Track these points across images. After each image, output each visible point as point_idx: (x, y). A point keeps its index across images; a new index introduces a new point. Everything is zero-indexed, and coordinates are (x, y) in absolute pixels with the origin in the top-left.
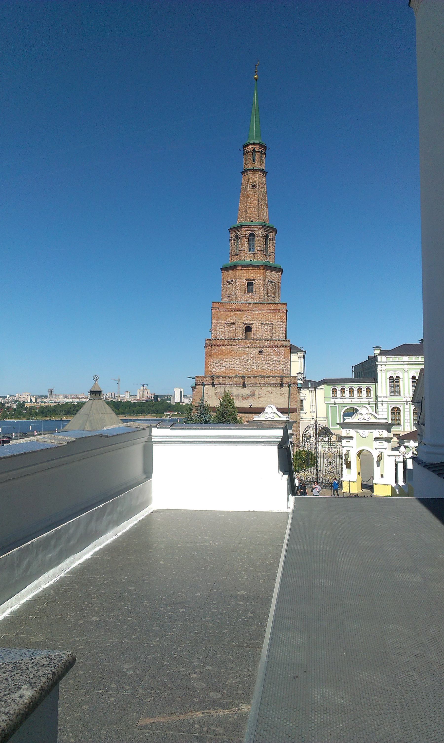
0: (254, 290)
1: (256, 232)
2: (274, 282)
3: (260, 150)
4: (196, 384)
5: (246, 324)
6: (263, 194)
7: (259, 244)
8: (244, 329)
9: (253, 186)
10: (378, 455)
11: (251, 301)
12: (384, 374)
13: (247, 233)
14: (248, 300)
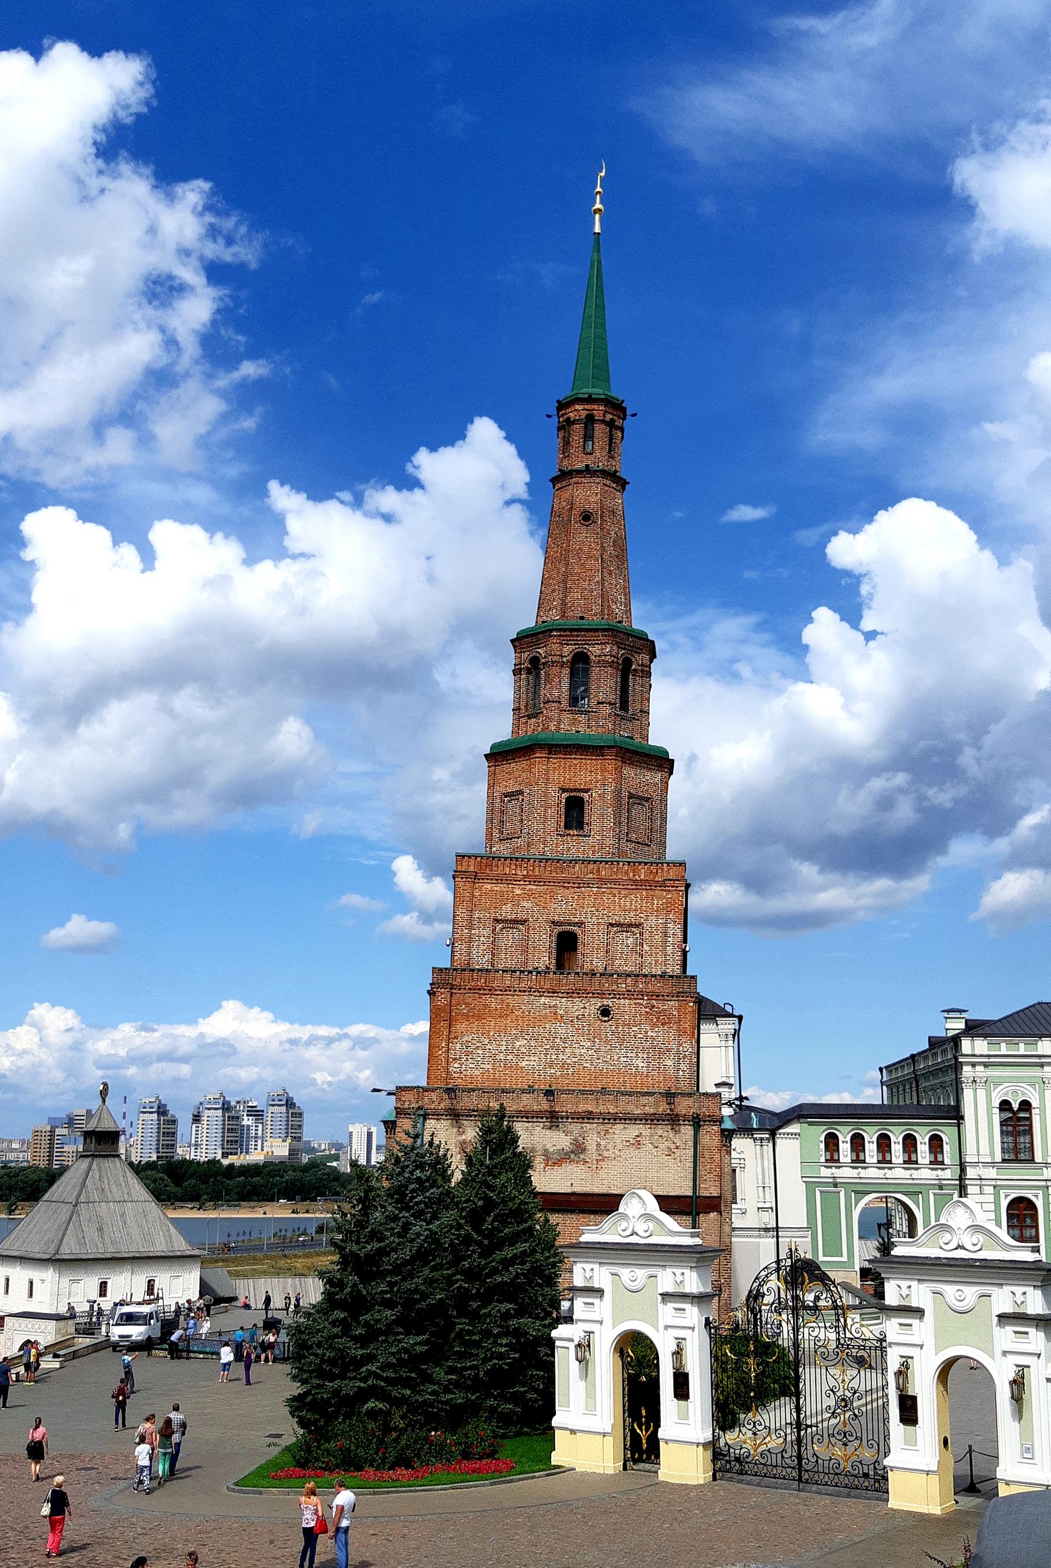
1: (594, 651)
4: (399, 1112)
6: (614, 541)
9: (587, 517)
10: (1011, 1376)
12: (981, 1093)
13: (567, 650)
14: (569, 849)
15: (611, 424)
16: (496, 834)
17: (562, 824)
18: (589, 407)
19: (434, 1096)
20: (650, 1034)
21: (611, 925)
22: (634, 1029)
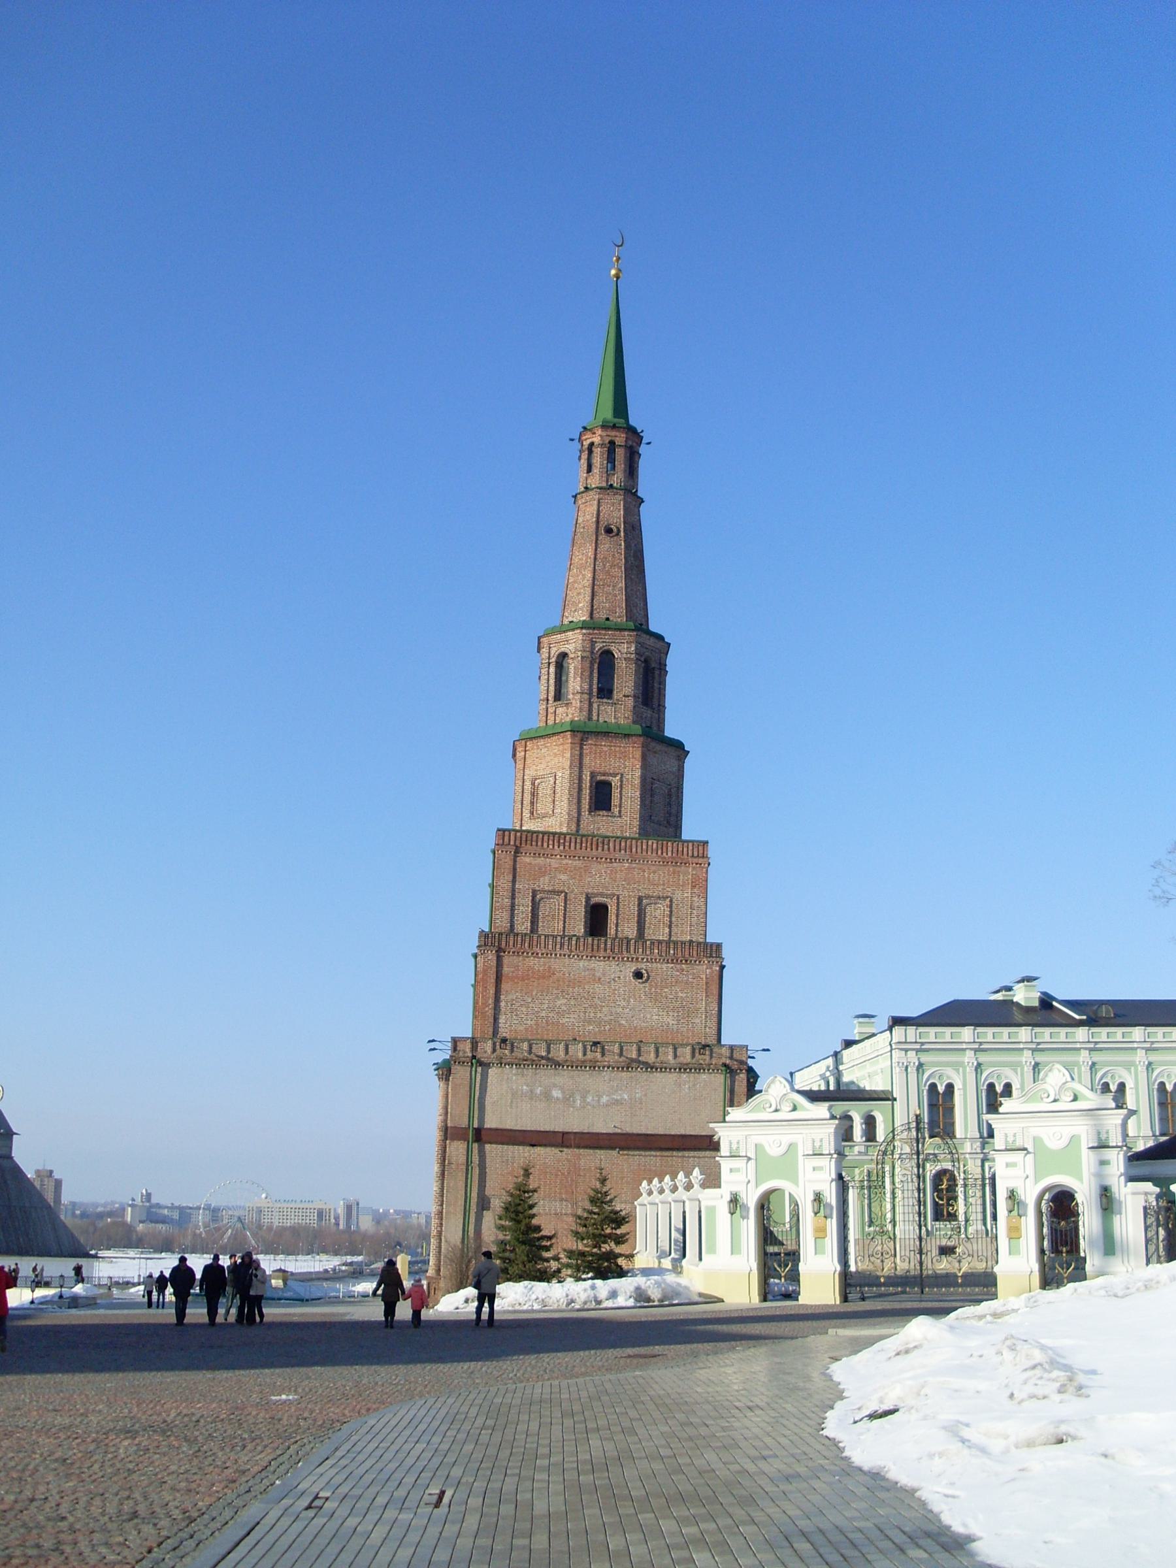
0: (615, 801)
3: (630, 443)
5: (597, 895)
7: (625, 682)
9: (609, 531)
13: (598, 646)
14: (599, 829)
16: (526, 814)
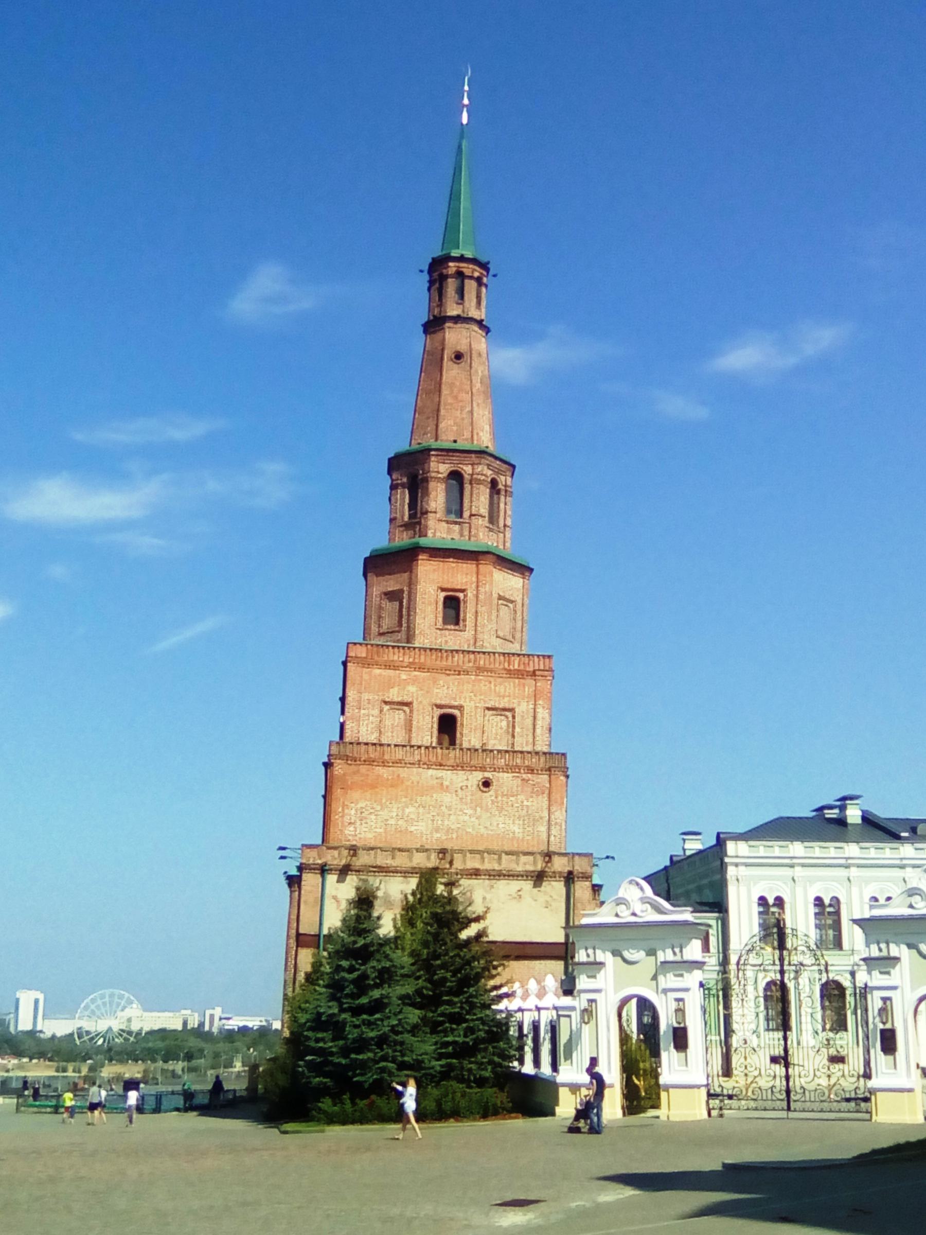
1: (467, 470)
2: (512, 602)
3: (476, 274)
8: (436, 720)
9: (458, 356)
11: (451, 646)
14: (446, 642)
15: (479, 280)
17: (440, 619)
18: (457, 264)
19: (336, 853)
20: (525, 803)
21: (488, 709)
22: (512, 799)
